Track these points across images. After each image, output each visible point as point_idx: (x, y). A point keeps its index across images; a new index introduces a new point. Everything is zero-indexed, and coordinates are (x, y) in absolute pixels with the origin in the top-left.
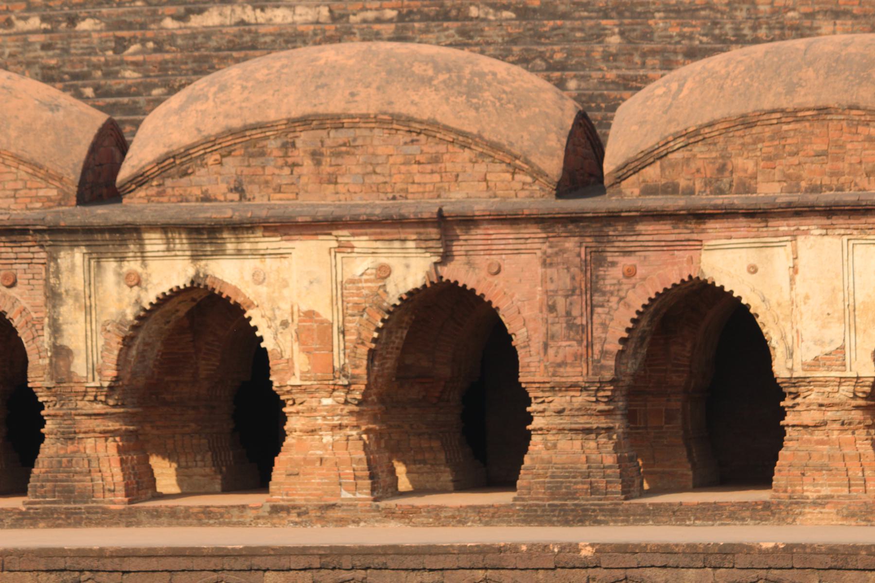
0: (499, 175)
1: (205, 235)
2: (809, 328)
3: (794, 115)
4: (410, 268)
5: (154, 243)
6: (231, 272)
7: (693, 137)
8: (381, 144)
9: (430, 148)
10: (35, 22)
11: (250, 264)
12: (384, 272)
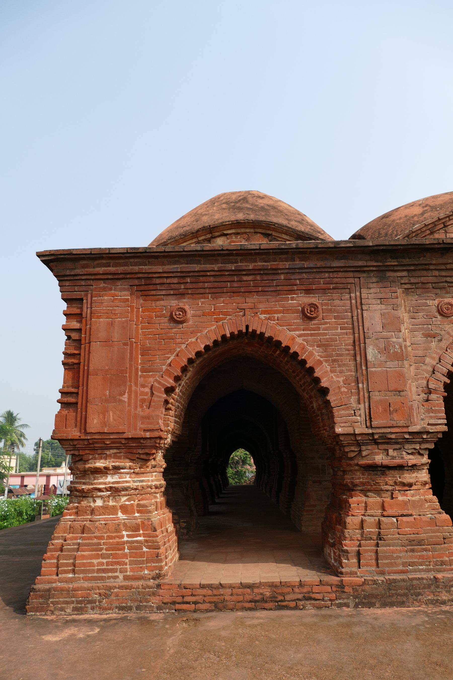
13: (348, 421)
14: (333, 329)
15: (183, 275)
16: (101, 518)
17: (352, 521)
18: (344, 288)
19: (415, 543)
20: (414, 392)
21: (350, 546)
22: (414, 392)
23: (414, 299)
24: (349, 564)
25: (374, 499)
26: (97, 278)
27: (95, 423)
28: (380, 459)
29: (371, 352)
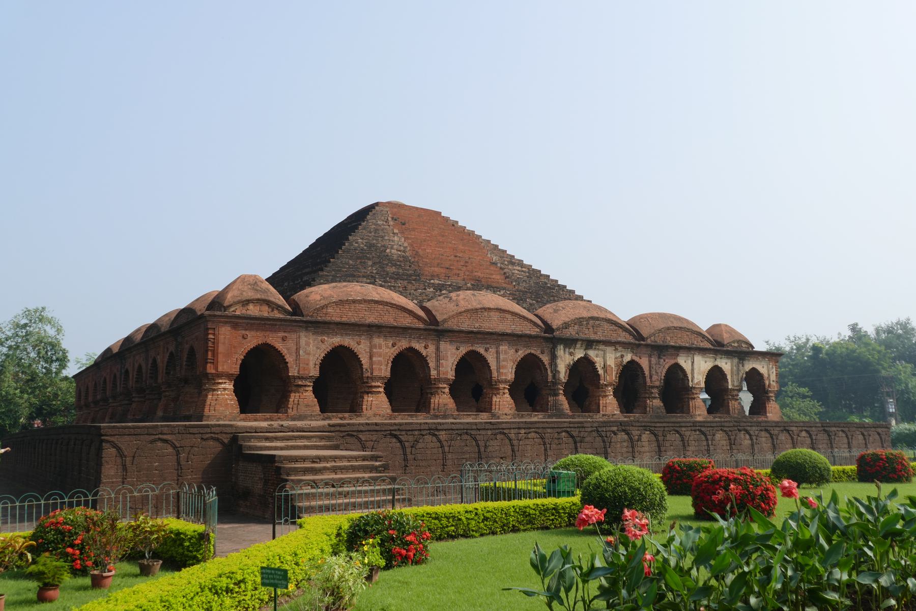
0: (627, 335)
1: (590, 344)
2: (695, 375)
3: (675, 328)
4: (628, 357)
5: (578, 346)
6: (592, 353)
7: (660, 331)
8: (606, 326)
9: (614, 327)
10: (432, 289)
11: (596, 352)
12: (622, 356)
13: (293, 372)
14: (291, 344)
15: (248, 324)
16: (221, 397)
17: (291, 400)
18: (295, 331)
19: (307, 406)
20: (311, 365)
21: (290, 406)
22: (311, 365)
23: (314, 337)
24: (290, 411)
25: (297, 394)
26: (220, 322)
27: (220, 369)
28: (300, 383)
29: (301, 352)
